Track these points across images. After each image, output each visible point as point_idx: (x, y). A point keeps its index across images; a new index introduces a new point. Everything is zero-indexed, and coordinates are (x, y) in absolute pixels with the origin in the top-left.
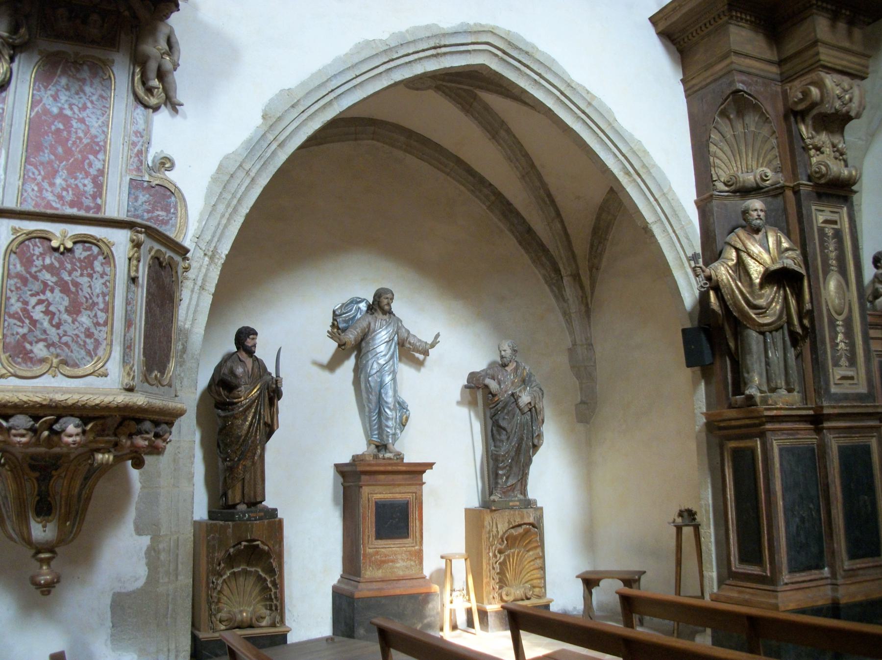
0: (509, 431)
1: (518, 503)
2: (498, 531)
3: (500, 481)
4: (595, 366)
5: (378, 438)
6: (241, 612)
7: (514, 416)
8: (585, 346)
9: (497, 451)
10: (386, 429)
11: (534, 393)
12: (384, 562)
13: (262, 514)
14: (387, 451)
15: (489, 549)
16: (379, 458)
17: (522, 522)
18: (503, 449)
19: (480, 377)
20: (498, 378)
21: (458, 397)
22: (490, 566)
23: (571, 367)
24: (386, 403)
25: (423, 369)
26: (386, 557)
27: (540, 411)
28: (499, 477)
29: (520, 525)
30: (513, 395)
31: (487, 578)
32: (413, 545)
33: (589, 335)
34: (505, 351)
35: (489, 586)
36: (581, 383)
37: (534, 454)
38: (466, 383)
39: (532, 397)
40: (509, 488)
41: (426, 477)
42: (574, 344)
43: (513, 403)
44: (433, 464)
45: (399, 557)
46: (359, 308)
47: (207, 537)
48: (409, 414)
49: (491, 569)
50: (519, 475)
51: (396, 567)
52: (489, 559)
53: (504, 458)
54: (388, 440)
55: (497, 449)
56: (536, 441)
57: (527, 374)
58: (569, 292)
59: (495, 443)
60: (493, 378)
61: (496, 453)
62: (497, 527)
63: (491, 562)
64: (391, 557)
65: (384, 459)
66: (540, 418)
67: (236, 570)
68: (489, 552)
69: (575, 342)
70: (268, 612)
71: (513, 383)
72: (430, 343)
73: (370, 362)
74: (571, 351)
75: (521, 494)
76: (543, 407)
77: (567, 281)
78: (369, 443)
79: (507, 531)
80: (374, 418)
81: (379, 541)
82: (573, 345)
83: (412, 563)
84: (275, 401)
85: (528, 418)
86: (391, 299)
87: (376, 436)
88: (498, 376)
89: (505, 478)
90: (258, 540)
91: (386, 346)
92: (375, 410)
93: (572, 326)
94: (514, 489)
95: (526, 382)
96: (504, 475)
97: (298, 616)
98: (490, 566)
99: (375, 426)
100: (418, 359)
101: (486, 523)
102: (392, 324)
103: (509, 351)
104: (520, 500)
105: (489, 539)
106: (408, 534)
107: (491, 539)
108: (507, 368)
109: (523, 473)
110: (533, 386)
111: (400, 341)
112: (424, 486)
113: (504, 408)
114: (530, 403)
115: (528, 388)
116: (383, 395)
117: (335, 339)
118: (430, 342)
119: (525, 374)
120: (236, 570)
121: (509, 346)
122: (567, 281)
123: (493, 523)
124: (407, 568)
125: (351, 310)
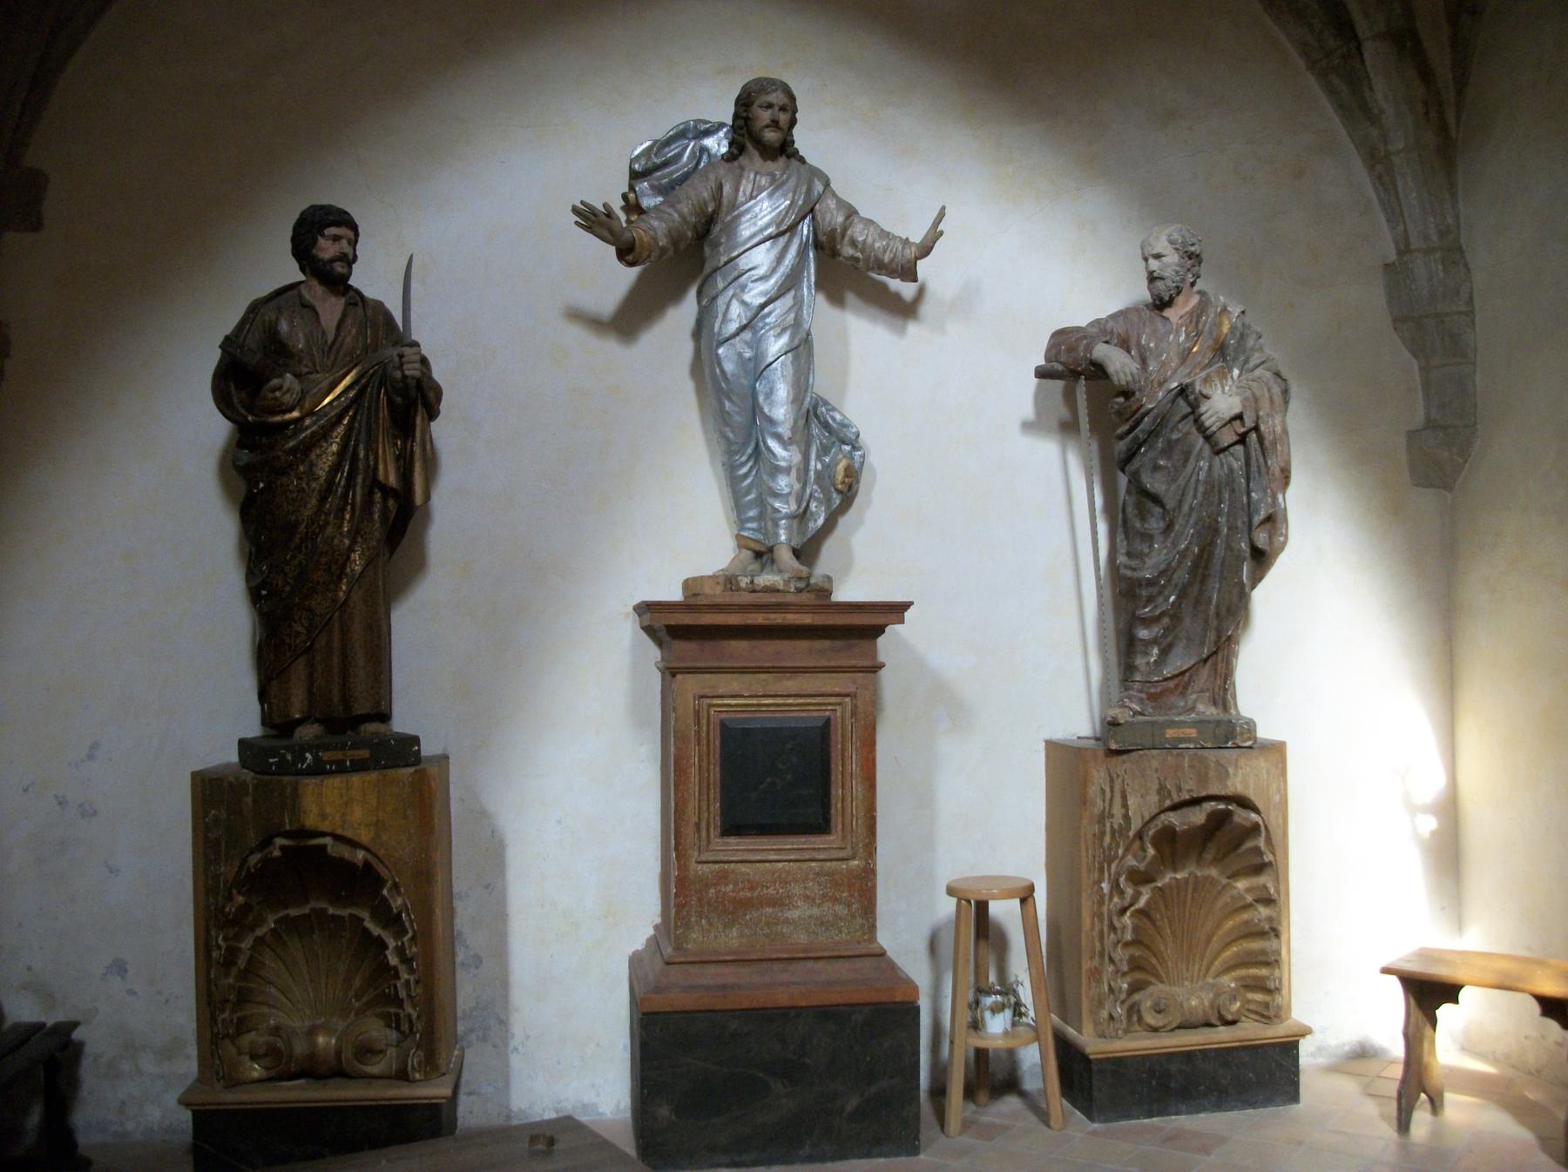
0: (1170, 504)
1: (1192, 732)
2: (1126, 817)
3: (1140, 661)
4: (1470, 313)
5: (758, 530)
6: (312, 1032)
7: (1186, 460)
8: (1438, 255)
9: (1134, 570)
10: (770, 500)
11: (1254, 384)
12: (747, 904)
13: (364, 753)
14: (775, 567)
15: (1101, 870)
16: (739, 589)
17: (1204, 794)
18: (1150, 562)
19: (1078, 340)
20: (1138, 344)
22: (1101, 921)
23: (1395, 321)
24: (771, 421)
25: (912, 328)
26: (752, 889)
27: (1274, 443)
28: (1140, 648)
29: (1195, 802)
30: (1183, 391)
31: (1092, 958)
32: (841, 854)
33: (1450, 220)
34: (1158, 256)
35: (1099, 981)
36: (1425, 370)
37: (1256, 579)
38: (1042, 362)
39: (1246, 399)
40: (1171, 684)
41: (885, 645)
42: (1404, 250)
43: (1185, 417)
44: (904, 607)
45: (796, 889)
46: (704, 150)
47: (204, 818)
48: (863, 456)
49: (1105, 929)
50: (1202, 644)
51: (787, 921)
52: (1101, 902)
53: (1154, 590)
54: (777, 535)
55: (1133, 563)
56: (1261, 539)
57: (1233, 328)
58: (1385, 90)
59: (1129, 544)
60: (1124, 344)
61: (1129, 573)
62: (1125, 805)
63: (1105, 909)
64: (771, 891)
65: (754, 591)
66: (1274, 464)
67: (293, 912)
68: (1100, 881)
69: (1408, 244)
70: (394, 1035)
71: (1185, 355)
72: (918, 241)
73: (721, 303)
74: (1396, 274)
75: (1215, 703)
76: (1285, 431)
77: (1374, 53)
78: (741, 542)
79: (1153, 818)
80: (744, 470)
81: (732, 840)
82: (1400, 253)
83: (841, 909)
84: (419, 421)
85: (1236, 465)
86: (783, 109)
87: (754, 525)
88: (1139, 337)
89: (1155, 651)
90: (324, 834)
91: (768, 250)
92: (746, 444)
93: (1397, 193)
94: (1188, 684)
95: (1230, 351)
96: (1154, 641)
97: (528, 1037)
98: (1101, 921)
99: (748, 493)
100: (897, 297)
101: (1093, 791)
102: (792, 183)
103: (1172, 258)
104: (1200, 723)
106: (827, 820)
107: (1107, 839)
108: (1168, 313)
109: (1219, 637)
110: (1252, 364)
111: (823, 239)
112: (882, 672)
113: (1153, 434)
114: (1240, 417)
115: (1236, 372)
116: (761, 399)
117: (596, 229)
118: (917, 237)
119: (1226, 329)
120: (293, 912)
121: (1171, 242)
122: (1374, 53)
123: (1112, 791)
124: (822, 924)
125: (680, 155)
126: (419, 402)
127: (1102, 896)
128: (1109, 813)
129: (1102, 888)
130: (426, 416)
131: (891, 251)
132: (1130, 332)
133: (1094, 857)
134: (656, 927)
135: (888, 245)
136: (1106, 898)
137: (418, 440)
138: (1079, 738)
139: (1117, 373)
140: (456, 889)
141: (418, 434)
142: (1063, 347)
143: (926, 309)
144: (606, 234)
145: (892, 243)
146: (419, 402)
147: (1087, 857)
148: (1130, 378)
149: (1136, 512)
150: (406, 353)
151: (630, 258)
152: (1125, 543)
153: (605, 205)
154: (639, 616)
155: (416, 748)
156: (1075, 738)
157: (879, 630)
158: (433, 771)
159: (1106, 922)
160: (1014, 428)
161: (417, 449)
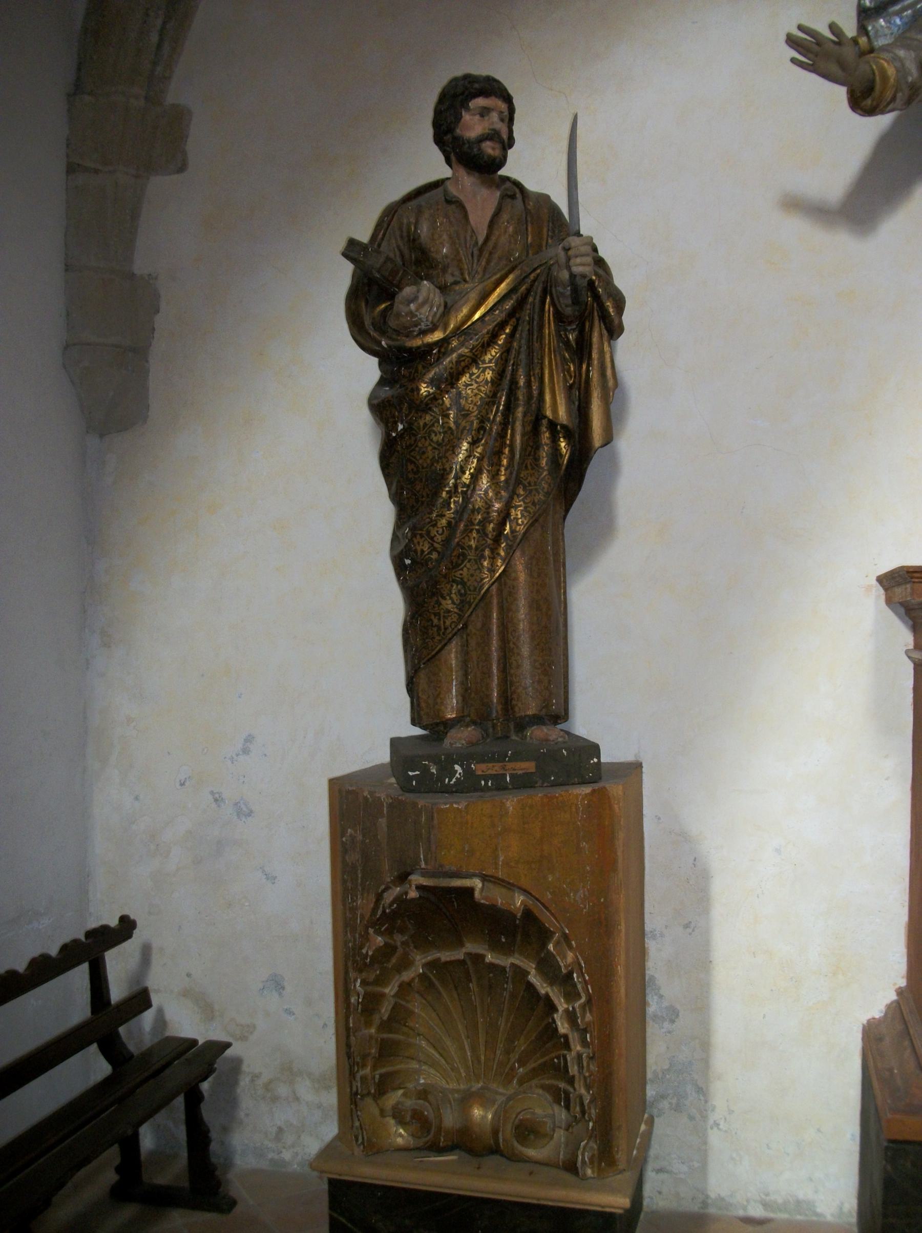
6: (467, 1099)
13: (529, 766)
47: (342, 837)
67: (446, 956)
70: (562, 1115)
84: (595, 339)
90: (473, 875)
97: (731, 1112)
120: (446, 956)
126: (596, 314)
130: (605, 332)
134: (900, 992)
137: (596, 362)
140: (648, 927)
141: (595, 355)
144: (834, 68)
146: (596, 314)
150: (573, 244)
151: (869, 102)
153: (833, 27)
154: (886, 590)
155: (596, 760)
158: (615, 789)
161: (594, 375)
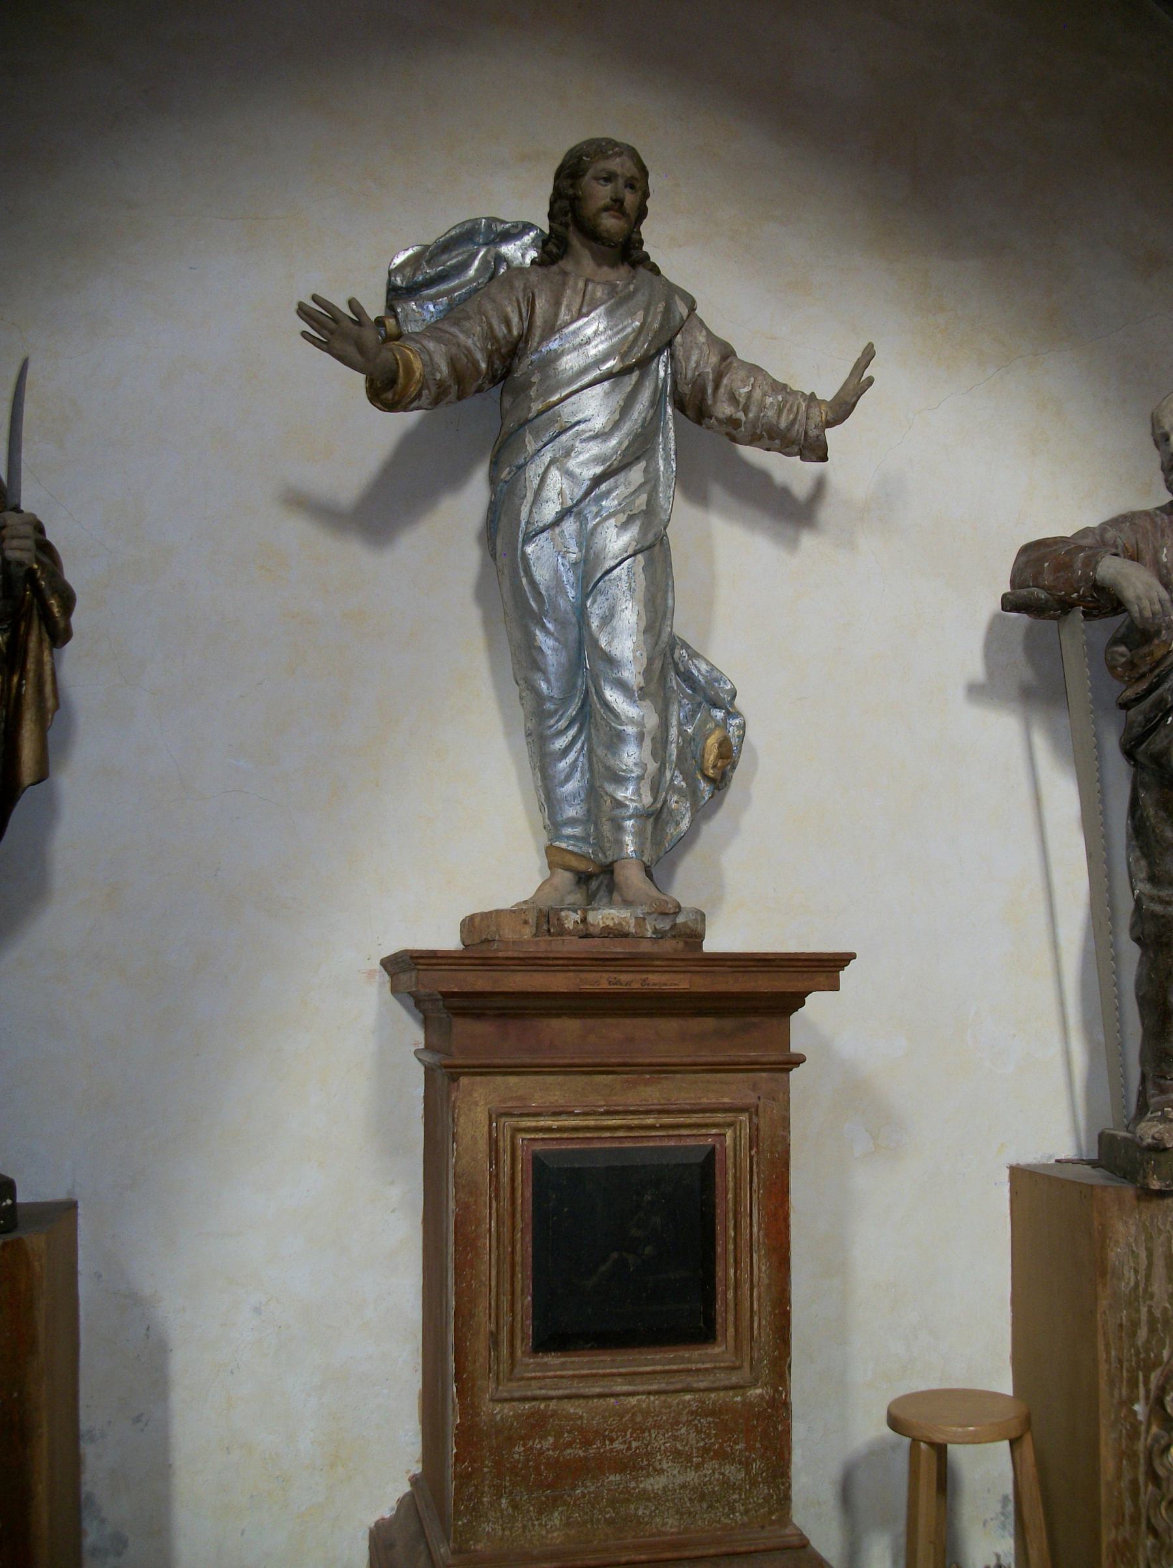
5: (584, 839)
10: (610, 788)
12: (580, 1470)
14: (616, 897)
15: (1133, 1384)
16: (562, 932)
21: (975, 667)
24: (610, 661)
25: (808, 541)
26: (586, 1443)
32: (734, 1379)
44: (843, 960)
46: (500, 259)
48: (743, 727)
51: (645, 1496)
52: (1134, 1435)
54: (620, 843)
59: (1151, 864)
61: (1158, 908)
63: (1141, 1446)
64: (617, 1445)
65: (587, 936)
68: (1133, 1400)
72: (829, 398)
73: (533, 472)
78: (554, 857)
80: (560, 743)
83: (733, 1472)
84: (33, 643)
86: (630, 184)
87: (577, 831)
91: (607, 394)
92: (565, 701)
98: (1135, 1466)
99: (568, 779)
100: (785, 493)
102: (641, 298)
105: (1133, 1335)
106: (710, 1321)
107: (1143, 1333)
111: (686, 389)
112: (795, 1074)
116: (595, 623)
117: (337, 345)
118: (827, 391)
124: (702, 1497)
125: (465, 265)
126: (35, 612)
127: (1135, 1425)
128: (1145, 1290)
129: (1135, 1413)
130: (46, 637)
131: (790, 410)
132: (1141, 545)
133: (1120, 1361)
134: (414, 1481)
135: (785, 401)
136: (1143, 1428)
137: (31, 675)
138: (1058, 1161)
139: (1139, 598)
140: (84, 1425)
141: (31, 665)
142: (1046, 564)
143: (827, 513)
144: (351, 351)
145: (791, 399)
146: (35, 612)
147: (1108, 1361)
148: (1157, 607)
149: (1162, 814)
150: (9, 522)
151: (389, 395)
152: (1143, 863)
153: (352, 303)
154: (392, 975)
155: (9, 1202)
156: (1053, 1161)
157: (796, 1001)
158: (35, 1241)
159: (1142, 1468)
160: (960, 693)
161: (28, 690)
